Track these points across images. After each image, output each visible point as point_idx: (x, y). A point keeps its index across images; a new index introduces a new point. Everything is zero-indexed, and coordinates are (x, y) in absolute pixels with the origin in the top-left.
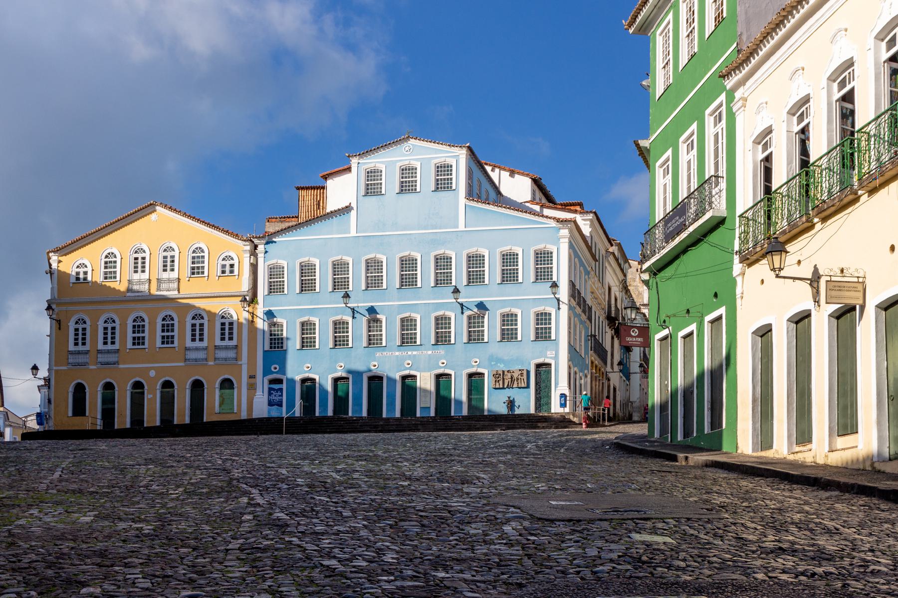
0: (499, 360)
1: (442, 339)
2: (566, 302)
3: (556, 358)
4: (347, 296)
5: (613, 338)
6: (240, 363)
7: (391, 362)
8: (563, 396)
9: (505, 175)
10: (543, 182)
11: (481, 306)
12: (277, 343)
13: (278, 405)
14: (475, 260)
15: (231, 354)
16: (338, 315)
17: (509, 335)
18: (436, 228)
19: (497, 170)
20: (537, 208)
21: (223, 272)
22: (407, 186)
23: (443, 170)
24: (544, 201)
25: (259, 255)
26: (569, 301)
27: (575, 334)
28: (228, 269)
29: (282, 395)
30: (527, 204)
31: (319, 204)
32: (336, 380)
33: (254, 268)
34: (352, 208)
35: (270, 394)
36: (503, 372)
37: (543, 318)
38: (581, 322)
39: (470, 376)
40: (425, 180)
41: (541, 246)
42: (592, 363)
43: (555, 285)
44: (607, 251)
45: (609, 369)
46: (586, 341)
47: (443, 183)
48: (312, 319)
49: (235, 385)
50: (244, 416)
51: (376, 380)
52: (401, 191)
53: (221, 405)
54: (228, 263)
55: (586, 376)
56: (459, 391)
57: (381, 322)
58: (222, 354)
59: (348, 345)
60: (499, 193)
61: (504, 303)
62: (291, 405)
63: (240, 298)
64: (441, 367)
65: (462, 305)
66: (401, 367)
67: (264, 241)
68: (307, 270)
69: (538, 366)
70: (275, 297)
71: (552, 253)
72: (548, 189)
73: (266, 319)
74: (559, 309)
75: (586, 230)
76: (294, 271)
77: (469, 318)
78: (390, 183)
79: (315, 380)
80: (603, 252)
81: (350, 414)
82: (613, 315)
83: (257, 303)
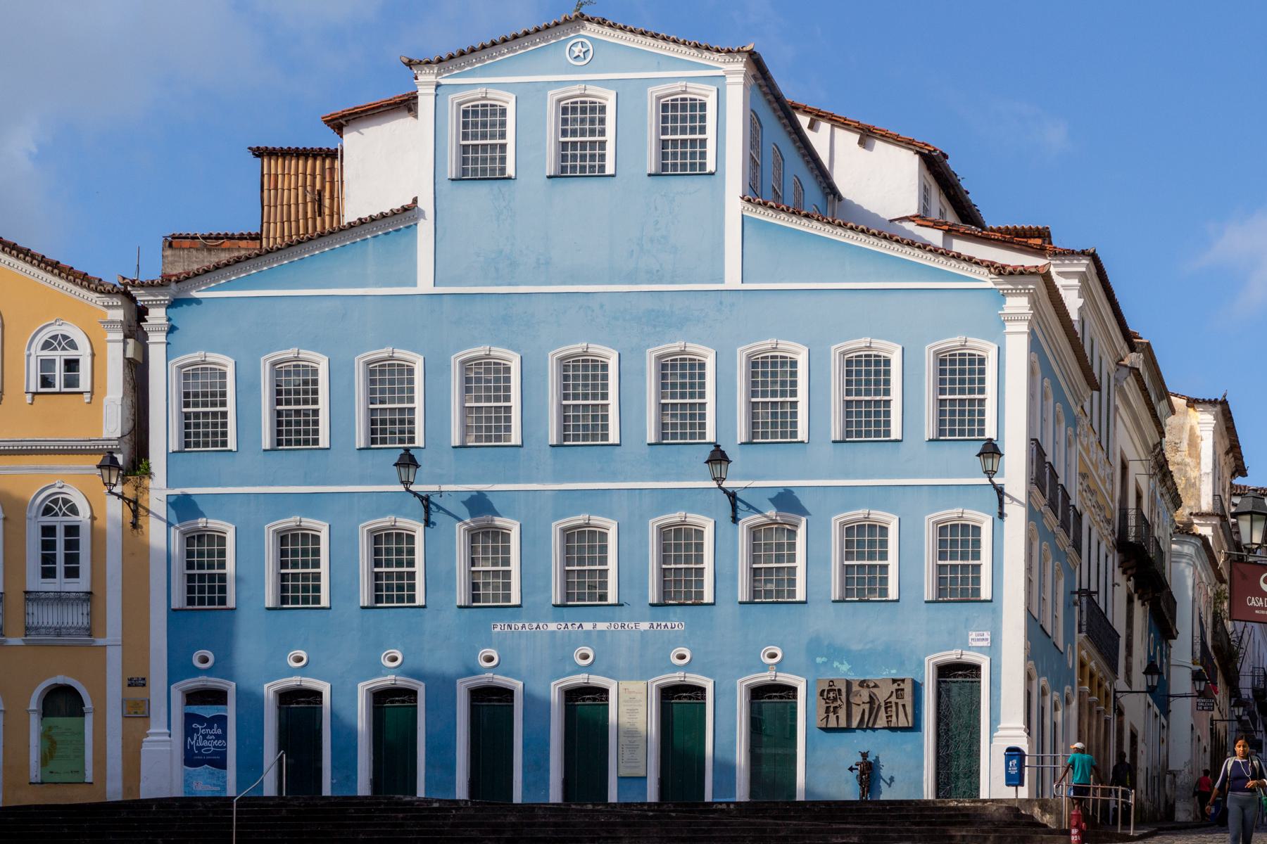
0: (837, 652)
1: (679, 589)
2: (1022, 496)
3: (994, 649)
4: (408, 461)
5: (1130, 600)
6: (100, 642)
7: (536, 656)
8: (1013, 753)
9: (847, 139)
10: (953, 164)
11: (786, 501)
12: (204, 586)
13: (212, 763)
14: (770, 374)
15: (75, 617)
16: (384, 515)
17: (863, 583)
18: (660, 281)
19: (825, 127)
20: (935, 237)
21: (46, 382)
22: (578, 159)
23: (682, 115)
24: (951, 218)
25: (153, 338)
26: (1030, 494)
27: (1042, 586)
28: (59, 373)
29: (224, 737)
30: (909, 226)
31: (324, 198)
32: (380, 698)
33: (137, 372)
34: (421, 214)
35: (189, 732)
36: (849, 684)
37: (957, 541)
38: (1059, 555)
39: (758, 693)
40: (629, 142)
41: (952, 342)
42: (1082, 665)
43: (991, 450)
44: (1119, 362)
45: (1121, 684)
46: (1069, 606)
47: (680, 155)
48: (308, 522)
49: (88, 705)
50: (114, 791)
52: (561, 174)
53: (45, 759)
54: (59, 356)
55: (1068, 702)
56: (727, 736)
57: (506, 537)
58: (48, 617)
59: (412, 598)
60: (830, 191)
61: (851, 496)
62: (251, 766)
63: (98, 459)
64: (676, 668)
65: (732, 496)
67: (164, 298)
68: (294, 391)
69: (945, 671)
70: (205, 459)
71: (982, 361)
72: (965, 185)
73: (173, 519)
74: (1001, 515)
75: (1073, 302)
76: (256, 387)
77: (754, 531)
78: (529, 145)
79: (318, 694)
80: (1108, 364)
81: (421, 793)
82: (1132, 539)
83: (148, 473)
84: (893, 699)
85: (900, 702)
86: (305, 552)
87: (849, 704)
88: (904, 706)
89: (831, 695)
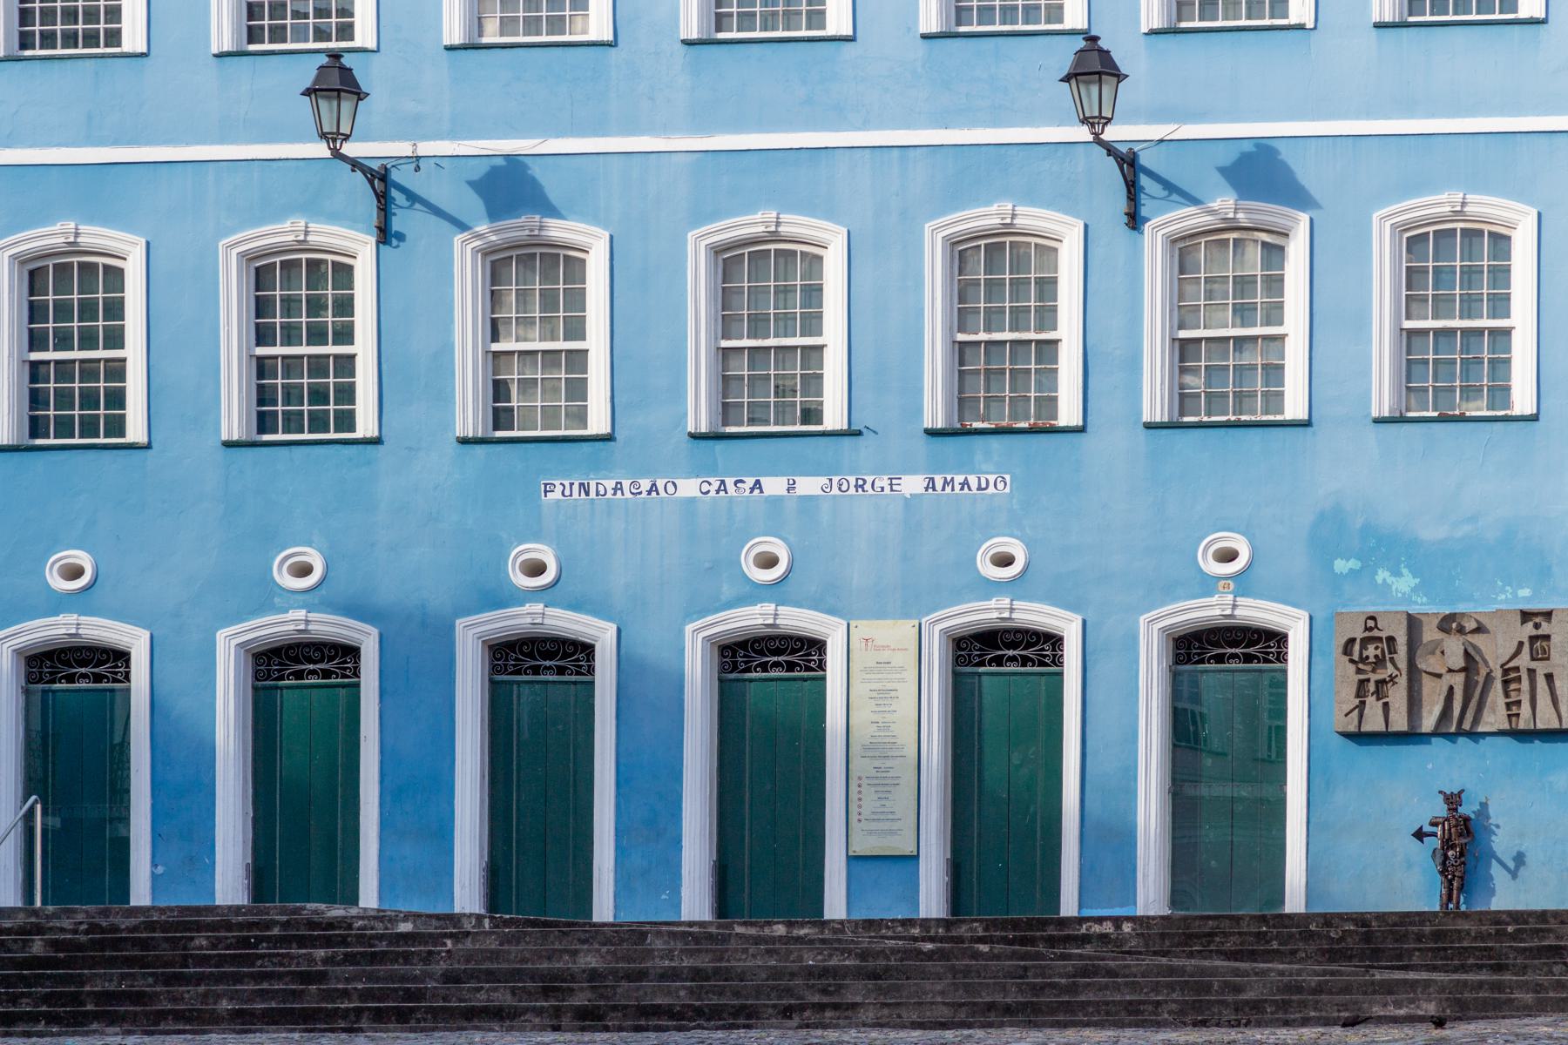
0: (1386, 548)
1: (998, 395)
4: (338, 84)
7: (648, 560)
11: (1260, 171)
16: (279, 216)
32: (274, 663)
36: (1413, 623)
39: (1193, 647)
48: (96, 236)
51: (540, 669)
56: (1115, 750)
57: (576, 268)
59: (346, 421)
61: (1423, 157)
64: (991, 588)
65: (1128, 162)
66: (712, 581)
77: (1183, 248)
81: (369, 897)
84: (1524, 661)
85: (1541, 668)
86: (88, 310)
87: (1413, 672)
88: (1549, 677)
89: (1371, 651)
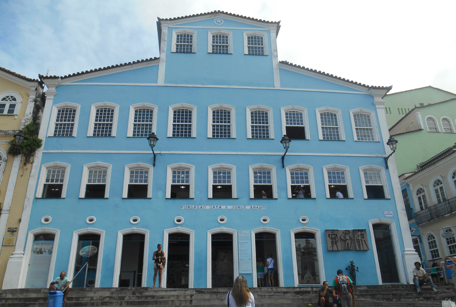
69: (376, 226)
84: (360, 238)
88: (364, 241)
